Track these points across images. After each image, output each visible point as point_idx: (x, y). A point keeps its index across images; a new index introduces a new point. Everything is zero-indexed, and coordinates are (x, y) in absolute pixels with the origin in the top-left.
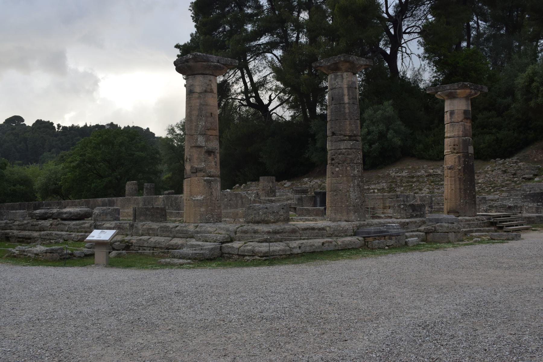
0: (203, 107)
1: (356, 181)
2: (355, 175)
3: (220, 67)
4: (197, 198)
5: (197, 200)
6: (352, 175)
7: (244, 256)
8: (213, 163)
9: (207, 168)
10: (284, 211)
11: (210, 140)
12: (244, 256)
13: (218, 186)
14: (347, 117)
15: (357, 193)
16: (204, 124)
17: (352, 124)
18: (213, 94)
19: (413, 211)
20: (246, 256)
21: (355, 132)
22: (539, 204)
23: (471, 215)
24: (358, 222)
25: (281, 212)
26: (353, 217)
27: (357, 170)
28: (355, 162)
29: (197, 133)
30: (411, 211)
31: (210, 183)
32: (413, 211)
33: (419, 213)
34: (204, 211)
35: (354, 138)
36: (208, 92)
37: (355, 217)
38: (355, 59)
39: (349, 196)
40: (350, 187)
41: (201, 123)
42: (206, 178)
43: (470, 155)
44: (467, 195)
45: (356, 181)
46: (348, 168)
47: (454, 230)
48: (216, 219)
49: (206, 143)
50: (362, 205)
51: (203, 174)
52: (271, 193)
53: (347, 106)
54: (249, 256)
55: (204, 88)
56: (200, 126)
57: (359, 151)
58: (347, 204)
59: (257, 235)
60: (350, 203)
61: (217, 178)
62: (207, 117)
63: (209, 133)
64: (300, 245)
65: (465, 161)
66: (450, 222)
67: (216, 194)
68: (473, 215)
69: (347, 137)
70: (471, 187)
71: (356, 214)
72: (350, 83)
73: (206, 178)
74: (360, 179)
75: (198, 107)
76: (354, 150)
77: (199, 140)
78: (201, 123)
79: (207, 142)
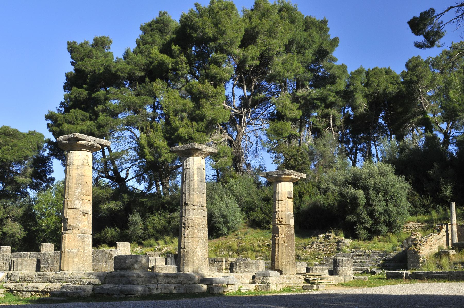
0: (80, 177)
1: (202, 241)
2: (201, 236)
3: (96, 146)
4: (72, 251)
5: (72, 252)
7: (113, 294)
11: (85, 204)
12: (113, 294)
14: (196, 191)
15: (202, 250)
16: (80, 190)
17: (199, 197)
18: (89, 167)
19: (246, 267)
20: (115, 294)
21: (202, 203)
22: (345, 268)
28: (201, 226)
29: (74, 197)
30: (244, 267)
31: (84, 238)
32: (246, 267)
33: (250, 269)
34: (77, 261)
35: (201, 207)
39: (196, 252)
40: (197, 245)
41: (78, 190)
43: (291, 226)
46: (196, 231)
48: (87, 268)
51: (78, 231)
53: (196, 183)
54: (116, 294)
55: (82, 162)
56: (77, 192)
59: (123, 279)
60: (197, 258)
63: (84, 198)
65: (288, 231)
69: (196, 207)
73: (80, 234)
74: (205, 240)
75: (76, 177)
76: (201, 217)
77: (75, 203)
78: (78, 190)
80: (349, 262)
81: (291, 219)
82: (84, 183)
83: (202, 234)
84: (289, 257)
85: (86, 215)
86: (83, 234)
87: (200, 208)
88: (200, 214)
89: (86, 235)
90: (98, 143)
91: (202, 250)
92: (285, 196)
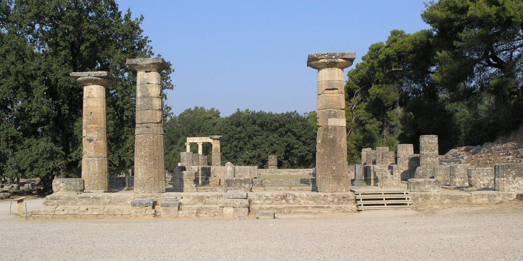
1: (142, 160)
2: (141, 155)
6: (139, 155)
8: (93, 148)
9: (88, 151)
10: (64, 184)
13: (95, 164)
15: (143, 170)
21: (144, 120)
22: (502, 179)
23: (327, 191)
24: (142, 194)
25: (61, 185)
26: (139, 190)
27: (144, 151)
36: (91, 98)
37: (140, 189)
38: (139, 61)
39: (138, 172)
42: (87, 159)
43: (330, 128)
44: (324, 170)
45: (142, 160)
46: (138, 150)
47: (232, 205)
48: (92, 188)
49: (88, 134)
50: (148, 180)
52: (404, 160)
55: (87, 95)
57: (148, 136)
58: (136, 179)
61: (95, 159)
62: (87, 116)
63: (89, 126)
64: (64, 209)
65: (323, 134)
66: (235, 197)
67: (93, 170)
68: (331, 190)
70: (330, 162)
71: (141, 187)
72: (142, 80)
76: (142, 135)
79: (88, 133)
80: (509, 170)
81: (330, 118)
82: (88, 114)
83: (143, 153)
84: (325, 170)
85: (92, 141)
86: (88, 158)
87: (144, 125)
88: (141, 133)
89: (91, 159)
90: (93, 76)
91: (143, 170)
92: (322, 88)
